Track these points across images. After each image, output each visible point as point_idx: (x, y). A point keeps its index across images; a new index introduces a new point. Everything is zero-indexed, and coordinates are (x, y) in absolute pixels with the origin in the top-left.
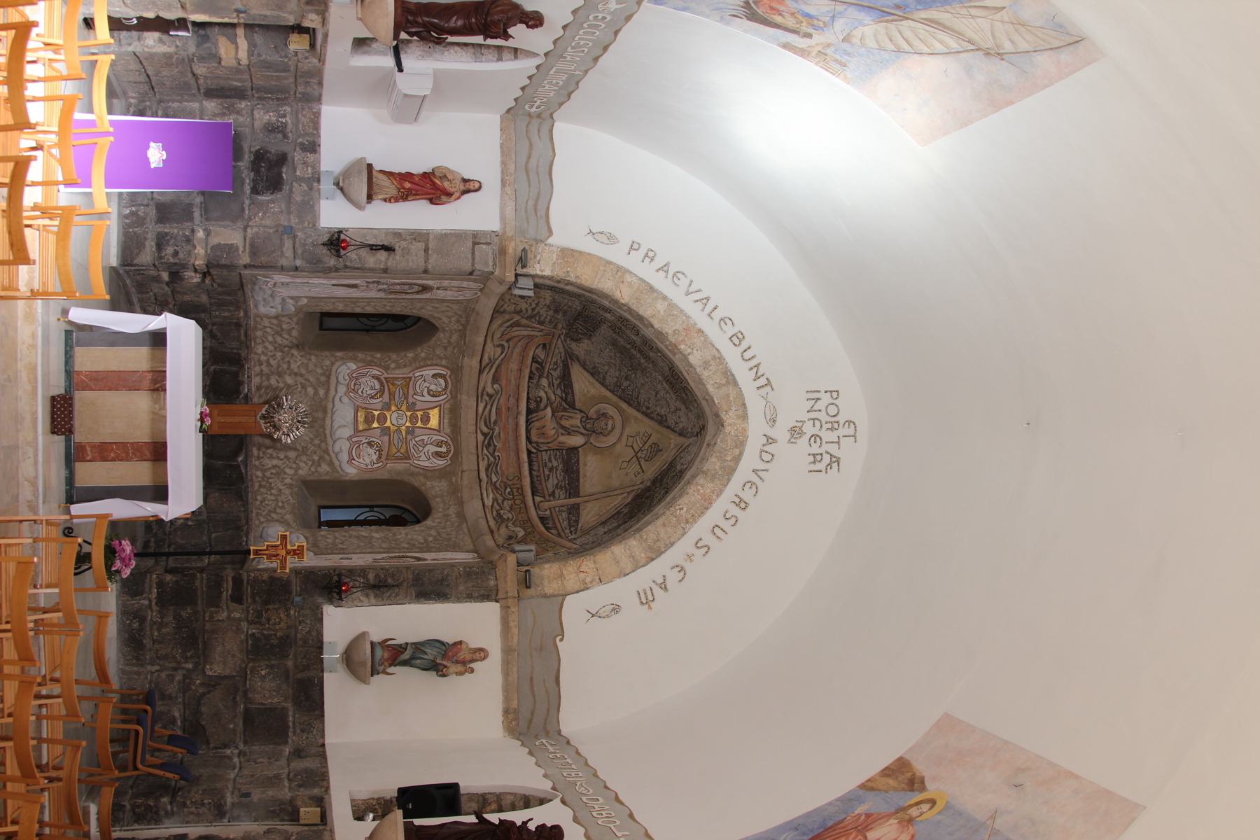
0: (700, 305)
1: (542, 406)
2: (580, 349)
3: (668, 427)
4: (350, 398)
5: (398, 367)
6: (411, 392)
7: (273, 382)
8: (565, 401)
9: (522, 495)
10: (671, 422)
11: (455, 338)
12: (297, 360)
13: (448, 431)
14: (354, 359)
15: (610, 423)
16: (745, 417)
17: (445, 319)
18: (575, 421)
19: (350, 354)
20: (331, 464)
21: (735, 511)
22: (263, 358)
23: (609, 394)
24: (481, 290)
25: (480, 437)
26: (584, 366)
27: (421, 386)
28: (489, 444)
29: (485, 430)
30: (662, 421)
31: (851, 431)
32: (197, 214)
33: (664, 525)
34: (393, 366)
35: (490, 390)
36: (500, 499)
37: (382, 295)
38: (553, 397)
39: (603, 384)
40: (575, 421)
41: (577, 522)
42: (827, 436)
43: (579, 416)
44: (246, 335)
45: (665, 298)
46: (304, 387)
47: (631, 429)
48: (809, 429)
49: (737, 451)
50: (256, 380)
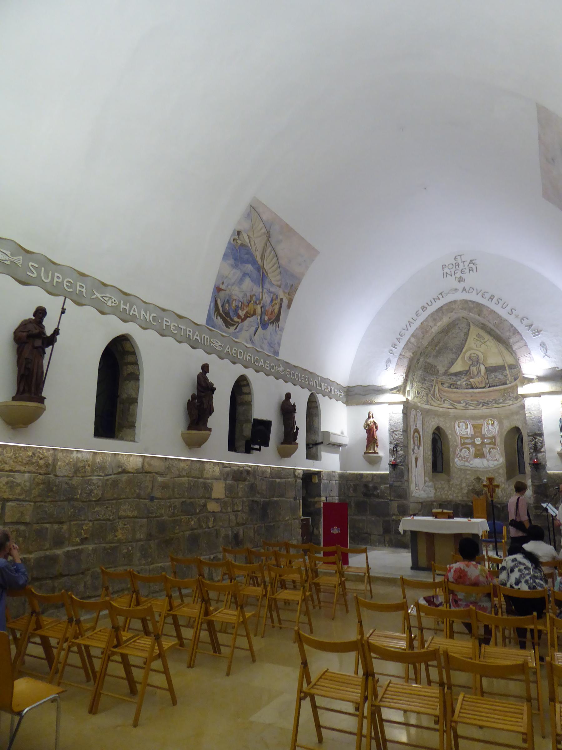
0: (412, 325)
1: (469, 383)
2: (442, 369)
3: (469, 331)
4: (471, 460)
5: (456, 441)
6: (467, 436)
7: (465, 491)
8: (466, 374)
9: (507, 389)
10: (466, 331)
11: (441, 419)
12: (455, 482)
13: (482, 421)
14: (453, 459)
15: (473, 355)
16: (455, 302)
17: (433, 423)
18: (474, 369)
19: (451, 461)
20: (499, 468)
21: (495, 300)
22: (455, 495)
23: (460, 356)
24: (416, 410)
25: (484, 407)
26: (449, 368)
28: (487, 404)
29: (481, 405)
30: (467, 334)
31: (459, 258)
32: (387, 519)
33: (503, 329)
34: (455, 443)
35: (464, 404)
36: (509, 398)
37: (421, 448)
38: (465, 379)
39: (457, 360)
40: (474, 369)
41: (514, 365)
42: (461, 266)
43: (472, 368)
44: (444, 502)
45: (410, 339)
46: (466, 479)
47: (474, 347)
48: (459, 275)
49: (470, 303)
50: (465, 499)
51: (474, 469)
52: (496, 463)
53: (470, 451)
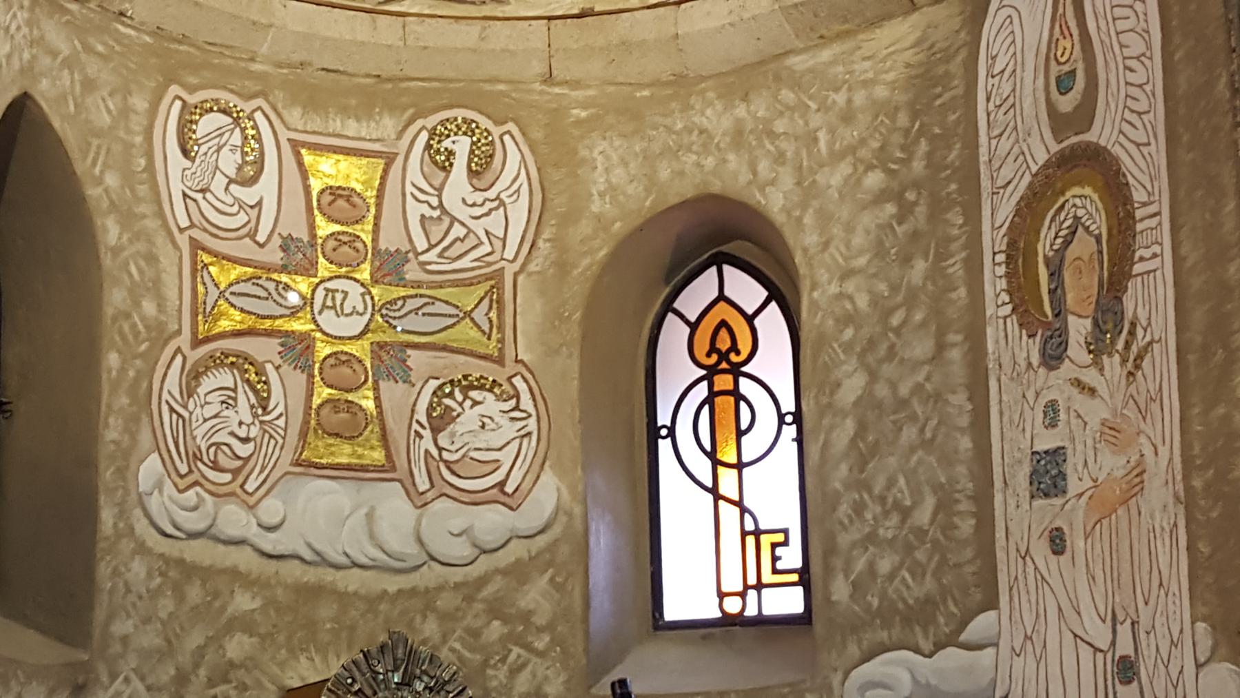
27: (223, 208)
51: (292, 571)
52: (491, 521)
53: (263, 403)
